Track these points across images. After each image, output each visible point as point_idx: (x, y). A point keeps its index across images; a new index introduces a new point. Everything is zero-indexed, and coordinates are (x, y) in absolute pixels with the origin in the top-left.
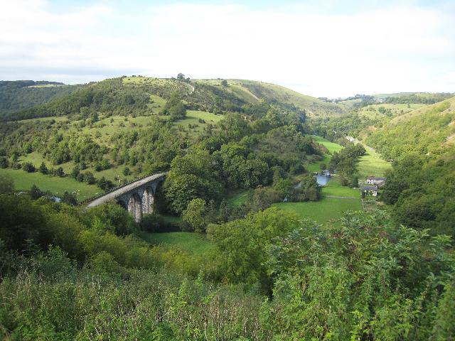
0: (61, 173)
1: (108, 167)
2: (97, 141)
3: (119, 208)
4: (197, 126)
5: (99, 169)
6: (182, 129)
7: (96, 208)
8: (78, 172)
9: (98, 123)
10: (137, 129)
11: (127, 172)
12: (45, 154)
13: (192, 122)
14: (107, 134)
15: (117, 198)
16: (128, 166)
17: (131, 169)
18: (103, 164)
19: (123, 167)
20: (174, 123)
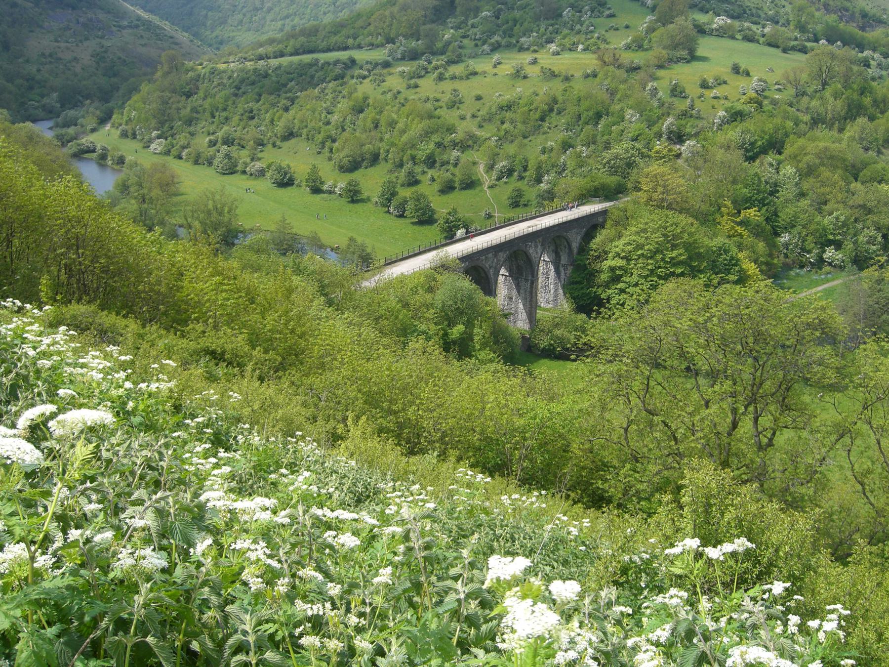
0: (354, 196)
1: (470, 184)
2: (450, 116)
3: (466, 284)
4: (725, 83)
5: (448, 188)
6: (677, 91)
7: (402, 280)
8: (394, 194)
9: (457, 69)
10: (557, 87)
11: (516, 202)
12: (323, 144)
13: (706, 70)
14: (479, 98)
15: (463, 259)
16: (519, 185)
17: (531, 193)
18: (458, 174)
19: (514, 184)
20: (661, 73)
